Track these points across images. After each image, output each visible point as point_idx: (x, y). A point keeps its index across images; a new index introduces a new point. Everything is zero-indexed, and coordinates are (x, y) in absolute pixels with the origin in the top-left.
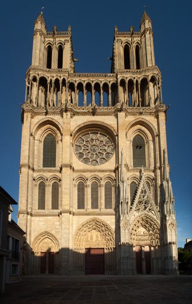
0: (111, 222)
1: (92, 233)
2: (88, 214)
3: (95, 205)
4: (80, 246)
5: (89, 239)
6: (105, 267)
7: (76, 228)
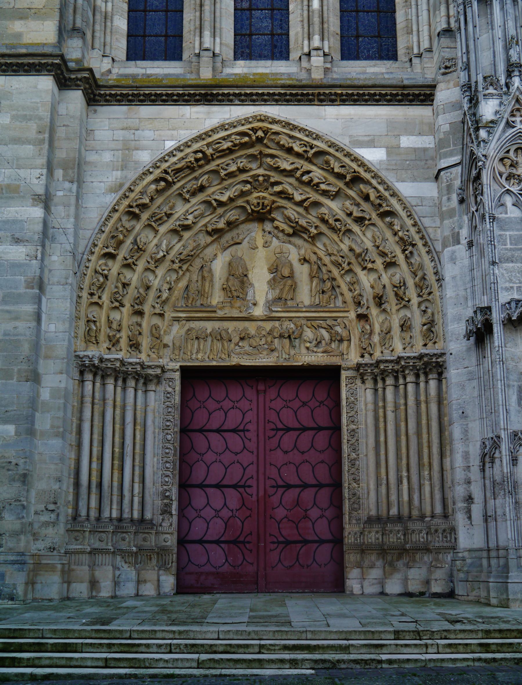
0: (392, 150)
1: (241, 250)
2: (207, 95)
3: (262, 27)
4: (135, 346)
5: (217, 298)
6: (350, 530)
7: (110, 199)
